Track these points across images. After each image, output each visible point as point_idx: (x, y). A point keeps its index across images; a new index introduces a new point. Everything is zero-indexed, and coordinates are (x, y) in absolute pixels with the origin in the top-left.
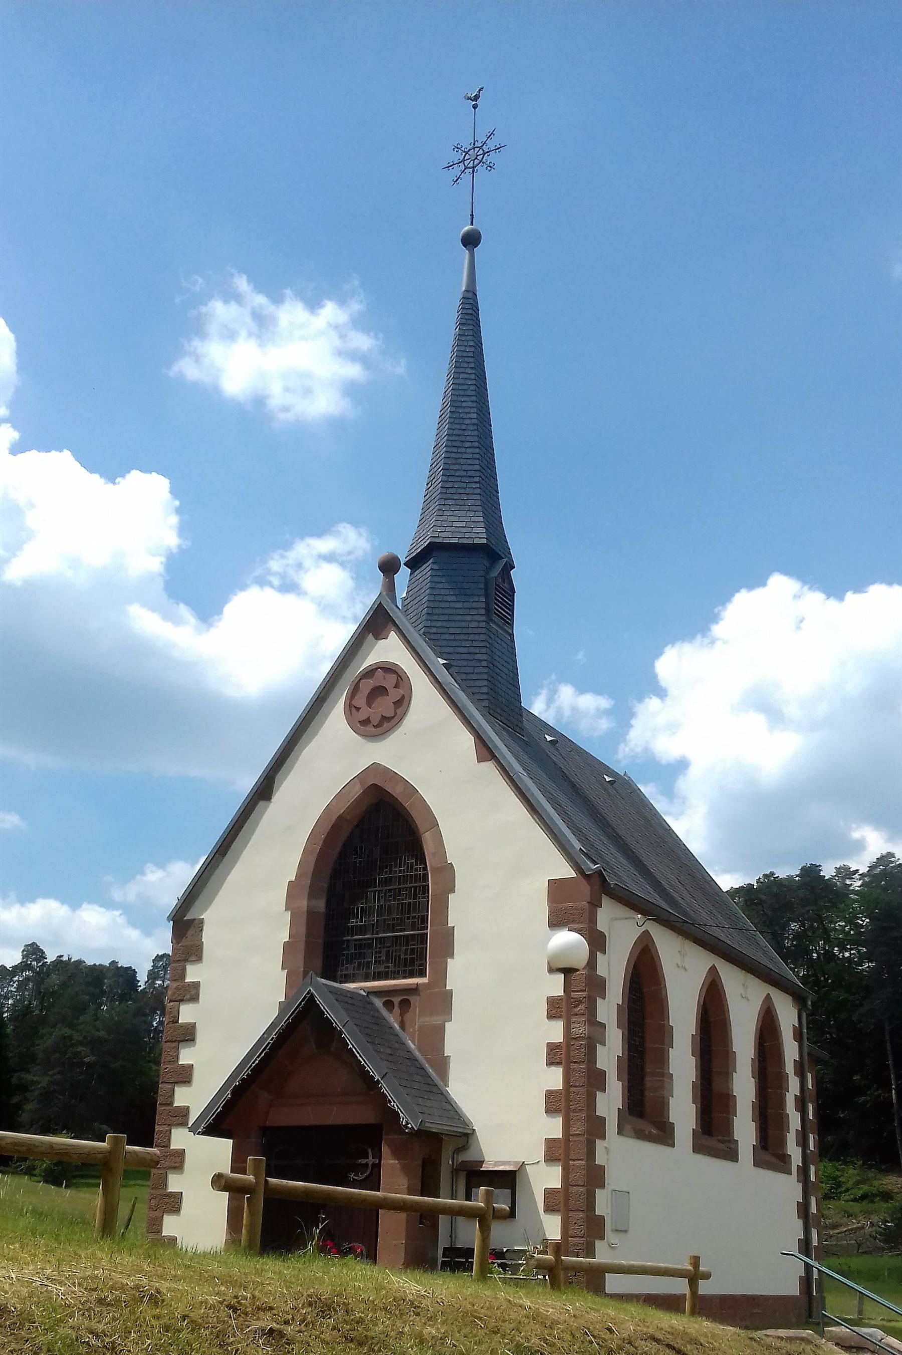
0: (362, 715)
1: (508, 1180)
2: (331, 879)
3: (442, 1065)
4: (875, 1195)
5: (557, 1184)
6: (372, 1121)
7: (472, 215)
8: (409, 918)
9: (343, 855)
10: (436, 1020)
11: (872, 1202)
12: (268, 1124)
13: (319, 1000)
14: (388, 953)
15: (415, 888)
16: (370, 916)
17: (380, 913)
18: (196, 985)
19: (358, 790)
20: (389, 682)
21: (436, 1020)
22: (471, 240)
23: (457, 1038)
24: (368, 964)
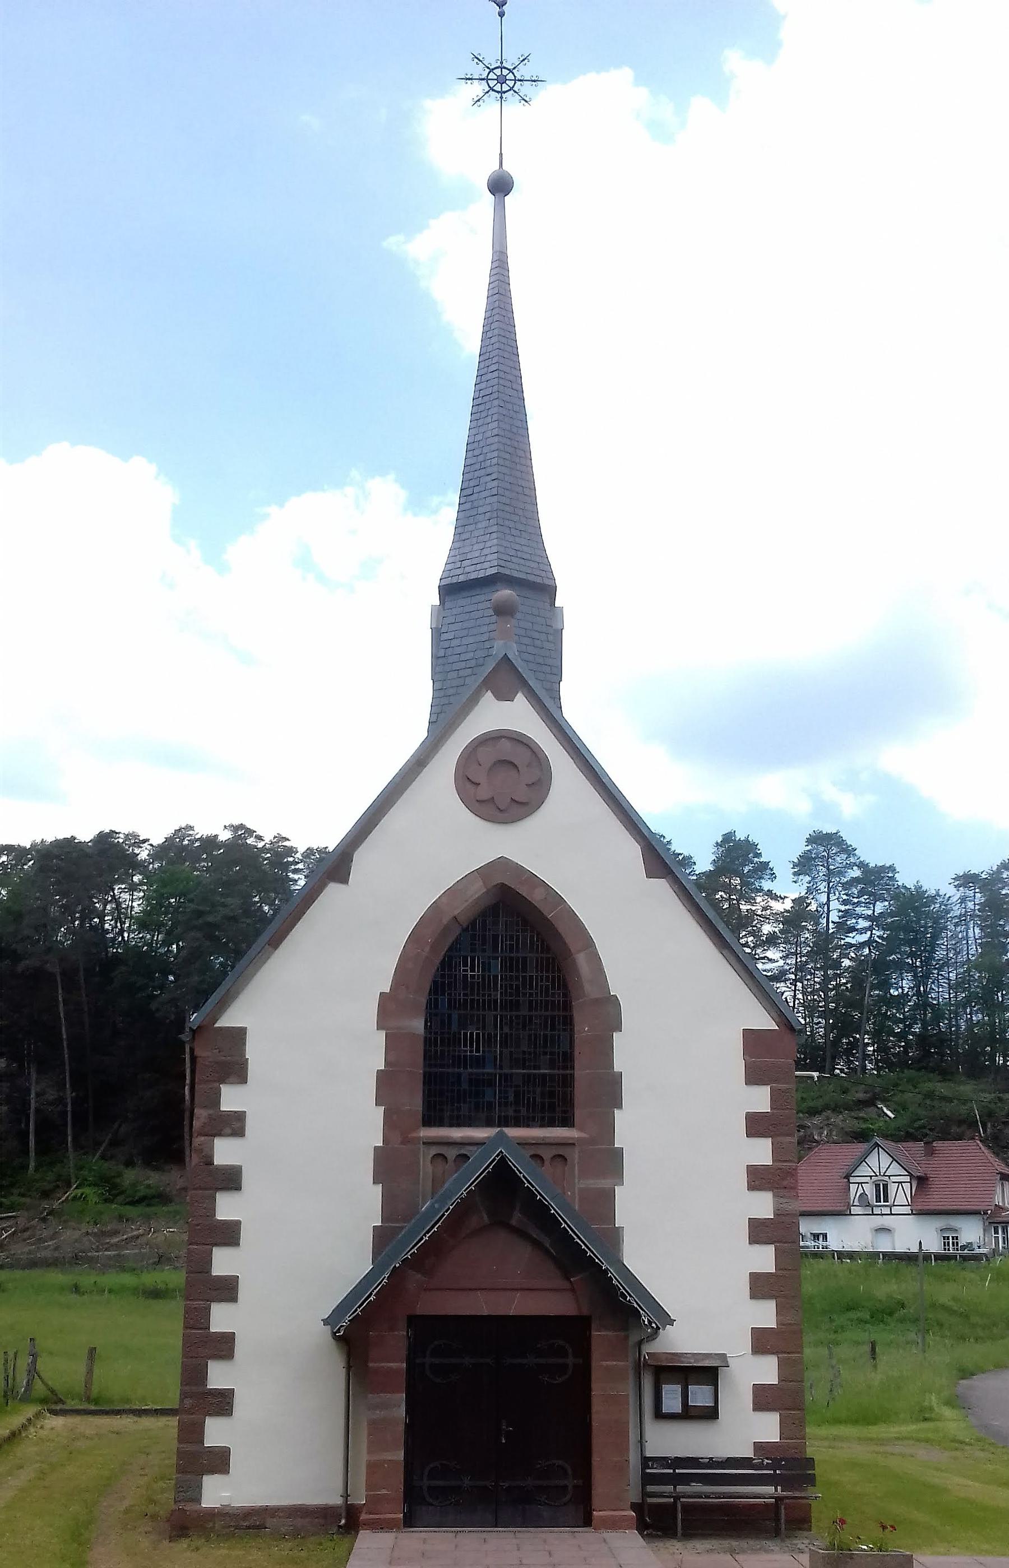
0: (484, 793)
1: (707, 1373)
2: (430, 994)
3: (613, 1238)
4: (154, 1197)
5: (773, 1379)
6: (574, 1314)
7: (501, 154)
8: (545, 1053)
9: (447, 964)
10: (604, 1183)
11: (149, 1205)
12: (419, 1311)
13: (513, 1162)
14: (517, 1095)
15: (553, 1018)
16: (489, 1046)
17: (504, 1043)
18: (240, 1117)
19: (477, 890)
20: (521, 757)
21: (604, 1183)
22: (500, 186)
23: (630, 1207)
24: (490, 1106)
